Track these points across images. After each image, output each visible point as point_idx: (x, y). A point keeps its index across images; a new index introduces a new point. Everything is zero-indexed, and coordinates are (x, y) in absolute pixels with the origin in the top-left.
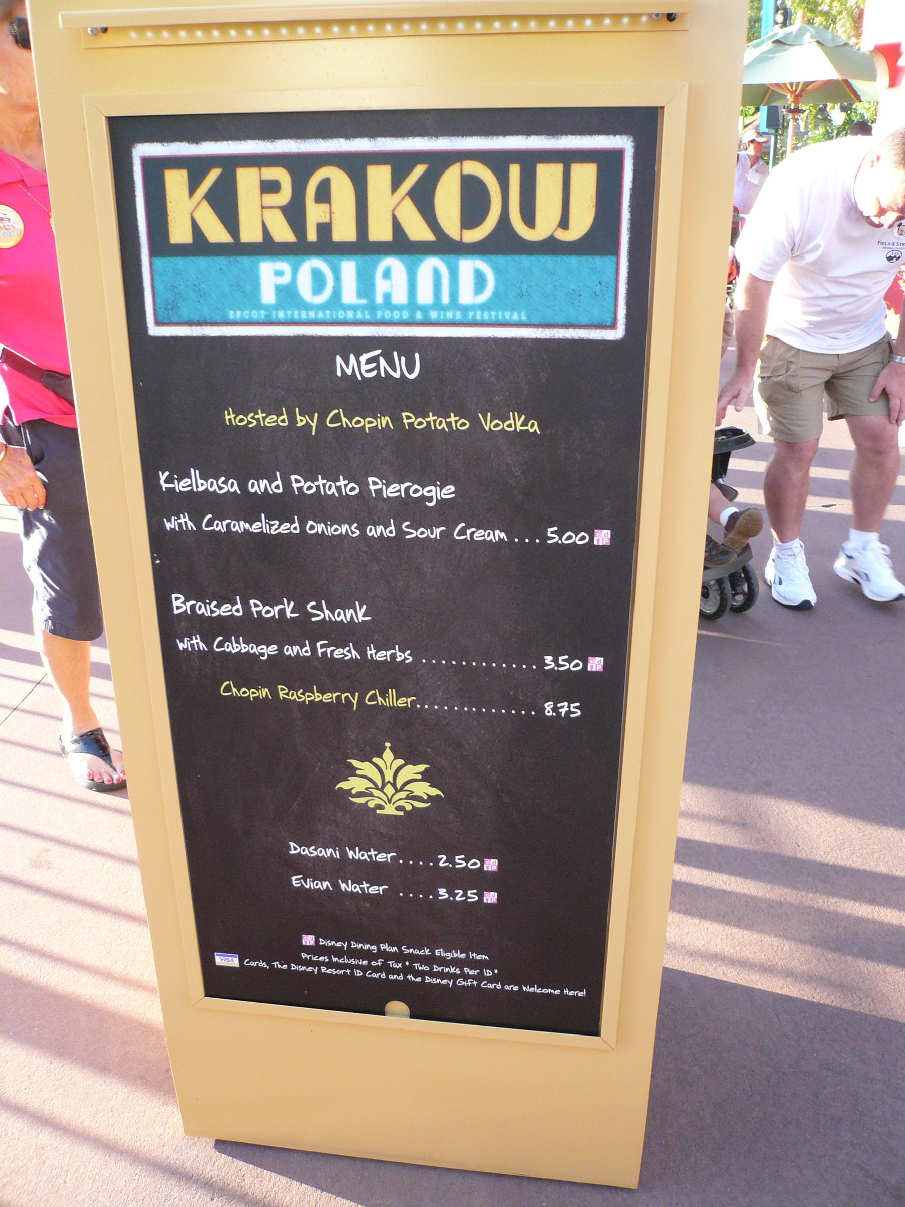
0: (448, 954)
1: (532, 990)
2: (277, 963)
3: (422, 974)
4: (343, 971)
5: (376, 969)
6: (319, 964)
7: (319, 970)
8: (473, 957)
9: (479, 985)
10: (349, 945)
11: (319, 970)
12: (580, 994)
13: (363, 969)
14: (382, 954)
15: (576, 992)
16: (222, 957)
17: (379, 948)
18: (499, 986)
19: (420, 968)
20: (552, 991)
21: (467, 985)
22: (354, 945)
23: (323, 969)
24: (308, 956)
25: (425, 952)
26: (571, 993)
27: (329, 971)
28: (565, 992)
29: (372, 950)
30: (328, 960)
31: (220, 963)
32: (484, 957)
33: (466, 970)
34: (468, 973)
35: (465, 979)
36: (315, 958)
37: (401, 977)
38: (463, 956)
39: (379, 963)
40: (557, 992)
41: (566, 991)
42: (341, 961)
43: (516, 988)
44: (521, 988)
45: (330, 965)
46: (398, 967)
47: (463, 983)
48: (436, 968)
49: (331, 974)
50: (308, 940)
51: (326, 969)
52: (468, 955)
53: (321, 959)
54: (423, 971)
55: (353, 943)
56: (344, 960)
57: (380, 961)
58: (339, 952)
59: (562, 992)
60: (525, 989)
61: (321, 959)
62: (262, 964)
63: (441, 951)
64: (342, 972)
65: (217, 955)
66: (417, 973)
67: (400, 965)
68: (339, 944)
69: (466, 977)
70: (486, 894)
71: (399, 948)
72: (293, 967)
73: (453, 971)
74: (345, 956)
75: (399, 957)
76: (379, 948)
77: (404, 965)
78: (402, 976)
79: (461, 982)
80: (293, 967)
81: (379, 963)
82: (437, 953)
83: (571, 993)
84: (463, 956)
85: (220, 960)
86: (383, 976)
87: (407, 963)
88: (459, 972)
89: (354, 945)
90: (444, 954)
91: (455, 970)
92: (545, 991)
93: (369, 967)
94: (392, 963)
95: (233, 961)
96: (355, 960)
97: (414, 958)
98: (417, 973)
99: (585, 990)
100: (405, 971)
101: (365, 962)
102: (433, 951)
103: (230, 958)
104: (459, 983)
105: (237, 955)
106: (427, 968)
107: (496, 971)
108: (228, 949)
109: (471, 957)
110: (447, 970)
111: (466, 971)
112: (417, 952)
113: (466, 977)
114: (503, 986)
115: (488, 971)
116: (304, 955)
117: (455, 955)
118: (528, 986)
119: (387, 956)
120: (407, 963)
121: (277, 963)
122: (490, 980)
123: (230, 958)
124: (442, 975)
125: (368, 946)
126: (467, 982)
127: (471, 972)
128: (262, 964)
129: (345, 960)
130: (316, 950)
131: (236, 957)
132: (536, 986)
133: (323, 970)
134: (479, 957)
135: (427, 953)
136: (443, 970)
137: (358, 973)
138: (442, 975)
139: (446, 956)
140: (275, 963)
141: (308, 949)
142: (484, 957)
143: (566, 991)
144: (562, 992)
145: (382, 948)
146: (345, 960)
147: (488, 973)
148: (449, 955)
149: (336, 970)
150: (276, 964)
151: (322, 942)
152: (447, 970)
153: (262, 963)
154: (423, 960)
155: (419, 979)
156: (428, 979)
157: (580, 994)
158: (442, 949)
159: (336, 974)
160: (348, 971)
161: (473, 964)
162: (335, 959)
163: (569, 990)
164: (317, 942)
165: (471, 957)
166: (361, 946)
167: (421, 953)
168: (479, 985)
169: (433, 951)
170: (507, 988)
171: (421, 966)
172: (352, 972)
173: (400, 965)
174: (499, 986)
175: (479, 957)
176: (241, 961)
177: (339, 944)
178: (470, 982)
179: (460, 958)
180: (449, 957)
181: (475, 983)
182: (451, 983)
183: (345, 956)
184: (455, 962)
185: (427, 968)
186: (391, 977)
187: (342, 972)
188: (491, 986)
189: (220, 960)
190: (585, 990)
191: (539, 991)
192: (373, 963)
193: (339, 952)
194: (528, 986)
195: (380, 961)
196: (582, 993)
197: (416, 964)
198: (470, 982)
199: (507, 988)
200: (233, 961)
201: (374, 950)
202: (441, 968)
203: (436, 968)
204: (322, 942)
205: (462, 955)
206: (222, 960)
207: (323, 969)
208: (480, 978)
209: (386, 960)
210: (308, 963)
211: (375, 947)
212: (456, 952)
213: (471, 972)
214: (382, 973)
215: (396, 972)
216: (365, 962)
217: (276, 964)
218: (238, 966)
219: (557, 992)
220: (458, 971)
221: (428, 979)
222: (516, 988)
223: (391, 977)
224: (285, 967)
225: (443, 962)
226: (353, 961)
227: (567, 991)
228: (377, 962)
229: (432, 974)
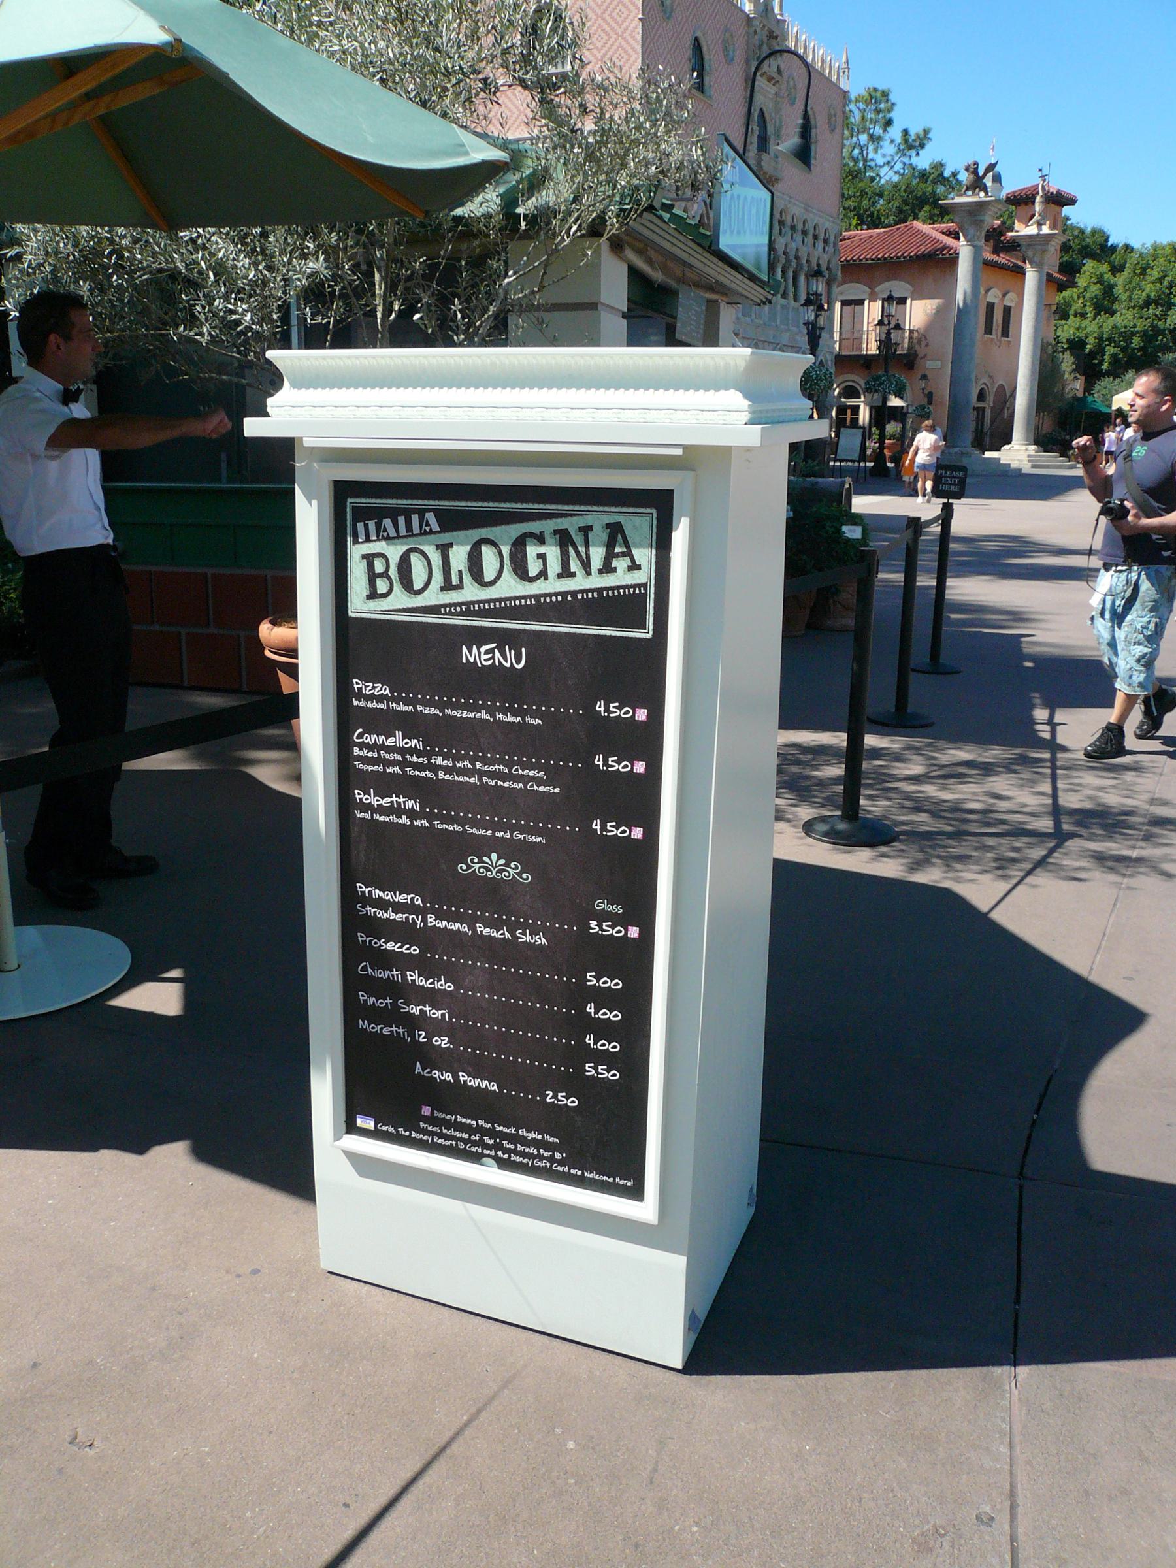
0: (529, 1134)
1: (591, 1176)
3: (508, 1151)
5: (475, 1144)
6: (432, 1134)
7: (433, 1139)
9: (551, 1166)
10: (456, 1118)
12: (629, 1184)
13: (465, 1142)
14: (480, 1130)
17: (477, 1123)
23: (436, 1139)
26: (622, 1182)
32: (556, 1140)
33: (542, 1151)
36: (430, 1128)
38: (540, 1137)
40: (611, 1180)
42: (449, 1133)
43: (579, 1173)
44: (583, 1173)
47: (539, 1163)
48: (520, 1148)
50: (426, 1111)
52: (543, 1137)
54: (509, 1149)
59: (614, 1180)
64: (449, 1143)
66: (506, 1151)
69: (542, 1158)
71: (493, 1126)
75: (492, 1133)
76: (477, 1123)
77: (495, 1141)
79: (537, 1163)
80: (414, 1134)
83: (622, 1182)
84: (540, 1137)
86: (480, 1150)
89: (460, 1119)
90: (526, 1134)
98: (506, 1151)
100: (497, 1147)
101: (466, 1136)
106: (512, 1146)
108: (367, 1114)
112: (505, 1130)
113: (542, 1158)
114: (569, 1170)
116: (422, 1124)
122: (561, 1163)
124: (524, 1154)
125: (469, 1121)
127: (547, 1154)
128: (391, 1129)
134: (552, 1140)
138: (524, 1154)
141: (426, 1120)
142: (556, 1140)
147: (558, 1156)
151: (436, 1114)
155: (506, 1156)
156: (513, 1157)
160: (454, 1143)
162: (445, 1131)
164: (432, 1113)
166: (464, 1120)
167: (509, 1131)
168: (551, 1166)
169: (517, 1130)
170: (573, 1172)
172: (457, 1144)
174: (566, 1170)
175: (552, 1140)
177: (448, 1117)
181: (548, 1164)
185: (512, 1146)
187: (449, 1143)
191: (596, 1177)
192: (473, 1138)
199: (573, 1172)
200: (370, 1124)
203: (520, 1148)
204: (436, 1114)
211: (474, 1122)
216: (466, 1136)
217: (401, 1130)
219: (611, 1180)
221: (513, 1157)
224: (407, 1133)
225: (525, 1142)
226: (458, 1134)
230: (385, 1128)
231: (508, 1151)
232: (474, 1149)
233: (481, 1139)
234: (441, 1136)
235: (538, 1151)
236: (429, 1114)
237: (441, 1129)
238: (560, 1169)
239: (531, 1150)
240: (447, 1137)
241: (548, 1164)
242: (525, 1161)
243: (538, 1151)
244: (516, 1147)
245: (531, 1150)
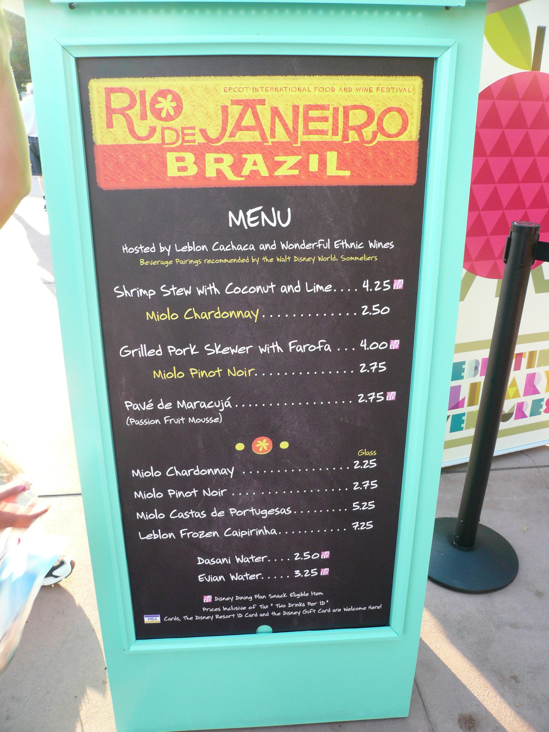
0: (298, 595)
1: (349, 610)
2: (186, 616)
3: (281, 610)
4: (230, 616)
6: (214, 613)
7: (214, 617)
8: (313, 594)
11: (214, 617)
12: (378, 608)
13: (243, 612)
15: (376, 607)
16: (149, 618)
17: (253, 597)
18: (329, 611)
19: (280, 607)
20: (361, 608)
21: (309, 613)
22: (237, 598)
23: (217, 616)
24: (207, 609)
25: (283, 596)
26: (373, 608)
27: (221, 617)
28: (369, 608)
29: (249, 599)
30: (220, 610)
31: (148, 622)
33: (309, 603)
34: (310, 605)
35: (308, 610)
36: (211, 610)
37: (268, 615)
38: (307, 595)
39: (254, 607)
40: (365, 608)
41: (370, 607)
42: (229, 610)
43: (339, 610)
44: (342, 610)
45: (220, 613)
46: (265, 608)
48: (290, 605)
49: (222, 619)
50: (208, 599)
51: (219, 616)
52: (310, 594)
53: (216, 610)
55: (237, 596)
56: (231, 608)
57: (254, 606)
58: (227, 604)
59: (367, 608)
60: (345, 610)
61: (216, 610)
62: (176, 619)
63: (293, 594)
65: (145, 617)
67: (267, 607)
68: (228, 599)
69: (308, 608)
70: (323, 553)
71: (267, 596)
72: (197, 618)
73: (300, 606)
74: (232, 606)
75: (266, 602)
76: (253, 597)
77: (269, 606)
78: (268, 614)
79: (305, 612)
80: (197, 618)
81: (254, 607)
82: (291, 596)
84: (307, 595)
85: (147, 620)
86: (256, 615)
87: (272, 605)
88: (304, 605)
89: (237, 598)
90: (295, 596)
91: (302, 604)
92: (357, 609)
93: (247, 611)
94: (262, 606)
95: (157, 619)
96: (238, 608)
97: (276, 601)
99: (381, 605)
100: (270, 610)
101: (244, 608)
102: (288, 595)
103: (155, 618)
104: (304, 612)
105: (159, 615)
107: (327, 601)
109: (312, 595)
110: (297, 605)
111: (308, 604)
112: (278, 596)
113: (308, 608)
115: (322, 602)
117: (302, 595)
118: (347, 608)
119: (258, 602)
120: (272, 605)
121: (186, 616)
122: (324, 608)
123: (155, 618)
124: (294, 609)
125: (246, 598)
126: (309, 611)
127: (312, 604)
128: (176, 619)
130: (213, 604)
131: (158, 616)
132: (352, 607)
133: (217, 617)
134: (317, 594)
135: (284, 596)
136: (294, 606)
137: (240, 616)
138: (294, 609)
139: (297, 597)
140: (185, 617)
141: (208, 605)
143: (370, 607)
144: (367, 608)
145: (256, 597)
147: (322, 603)
148: (299, 595)
149: (225, 616)
150: (186, 617)
151: (217, 599)
152: (297, 605)
153: (176, 618)
154: (282, 601)
155: (279, 614)
156: (285, 613)
157: (378, 608)
158: (294, 593)
159: (225, 618)
160: (233, 615)
162: (225, 609)
163: (372, 606)
164: (213, 599)
165: (312, 595)
166: (242, 598)
167: (281, 597)
168: (316, 612)
169: (288, 595)
170: (334, 611)
171: (280, 605)
172: (236, 616)
173: (267, 607)
174: (329, 611)
176: (162, 619)
177: (228, 599)
178: (311, 611)
179: (305, 596)
180: (298, 597)
181: (314, 611)
182: (299, 614)
183: (232, 606)
184: (303, 599)
186: (262, 615)
188: (324, 611)
189: (147, 620)
190: (381, 605)
192: (250, 608)
193: (227, 604)
194: (347, 608)
195: (254, 606)
196: (380, 607)
197: (277, 605)
198: (311, 611)
199: (334, 611)
200: (157, 619)
201: (251, 599)
202: (293, 605)
203: (290, 605)
204: (217, 599)
205: (306, 594)
206: (149, 620)
207: (217, 616)
208: (317, 607)
209: (258, 605)
211: (251, 598)
212: (303, 593)
213: (312, 604)
214: (255, 614)
215: (265, 611)
216: (244, 608)
217: (186, 617)
218: (160, 622)
219: (365, 608)
220: (304, 605)
221: (285, 613)
222: (339, 610)
223: (262, 615)
224: (191, 618)
225: (295, 600)
226: (237, 609)
227: (371, 607)
228: (253, 607)
229: (287, 609)
230: (170, 619)
232: (251, 616)
235: (306, 604)
236: (210, 600)
237: (222, 609)
238: (324, 611)
240: (226, 613)
241: (314, 611)
243: (306, 604)
244: (287, 605)
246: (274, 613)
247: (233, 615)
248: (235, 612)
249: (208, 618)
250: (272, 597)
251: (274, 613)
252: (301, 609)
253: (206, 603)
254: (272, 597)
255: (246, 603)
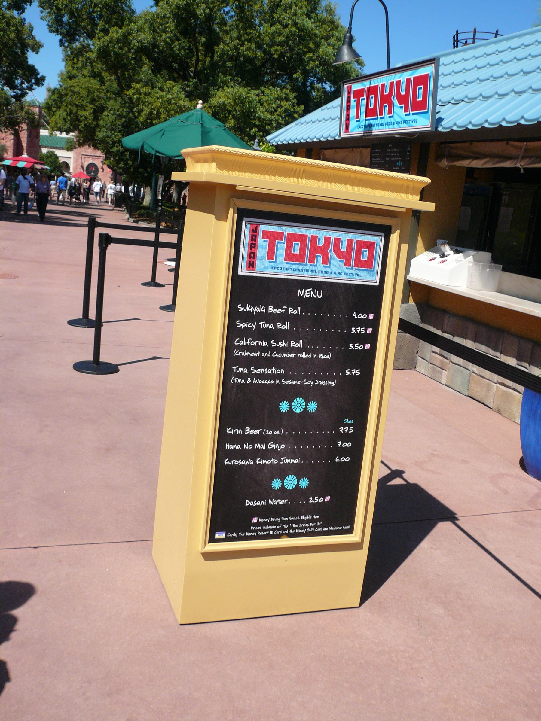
3: (295, 529)
5: (278, 530)
7: (257, 533)
13: (273, 530)
23: (259, 533)
27: (260, 534)
33: (311, 524)
35: (310, 528)
36: (256, 529)
42: (266, 528)
43: (327, 529)
44: (329, 529)
48: (301, 525)
54: (296, 527)
58: (265, 524)
61: (258, 528)
64: (265, 533)
69: (310, 527)
72: (247, 534)
79: (308, 530)
100: (289, 529)
101: (275, 527)
106: (297, 526)
110: (304, 525)
116: (252, 528)
119: (283, 522)
122: (319, 527)
124: (302, 528)
128: (235, 535)
129: (268, 527)
137: (272, 532)
138: (302, 528)
146: (268, 527)
147: (318, 524)
152: (304, 525)
154: (297, 522)
155: (294, 531)
156: (297, 531)
160: (268, 532)
161: (313, 521)
162: (264, 528)
168: (314, 530)
170: (324, 529)
174: (321, 529)
185: (297, 526)
186: (284, 532)
187: (265, 533)
188: (319, 530)
192: (278, 527)
193: (265, 524)
199: (324, 529)
203: (301, 525)
207: (259, 533)
208: (315, 527)
209: (283, 525)
210: (254, 531)
215: (286, 529)
216: (275, 527)
217: (240, 534)
220: (308, 525)
221: (297, 531)
223: (284, 532)
224: (244, 534)
226: (270, 527)
229: (299, 528)
230: (231, 535)
231: (295, 529)
232: (278, 533)
233: (282, 527)
234: (261, 531)
235: (309, 524)
237: (262, 527)
239: (307, 525)
241: (313, 529)
242: (303, 531)
243: (309, 524)
244: (299, 525)
245: (307, 525)
246: (291, 531)
247: (268, 532)
248: (269, 530)
249: (253, 534)
250: (291, 519)
251: (291, 531)
252: (306, 528)
253: (254, 523)
254: (291, 519)
255: (276, 523)
